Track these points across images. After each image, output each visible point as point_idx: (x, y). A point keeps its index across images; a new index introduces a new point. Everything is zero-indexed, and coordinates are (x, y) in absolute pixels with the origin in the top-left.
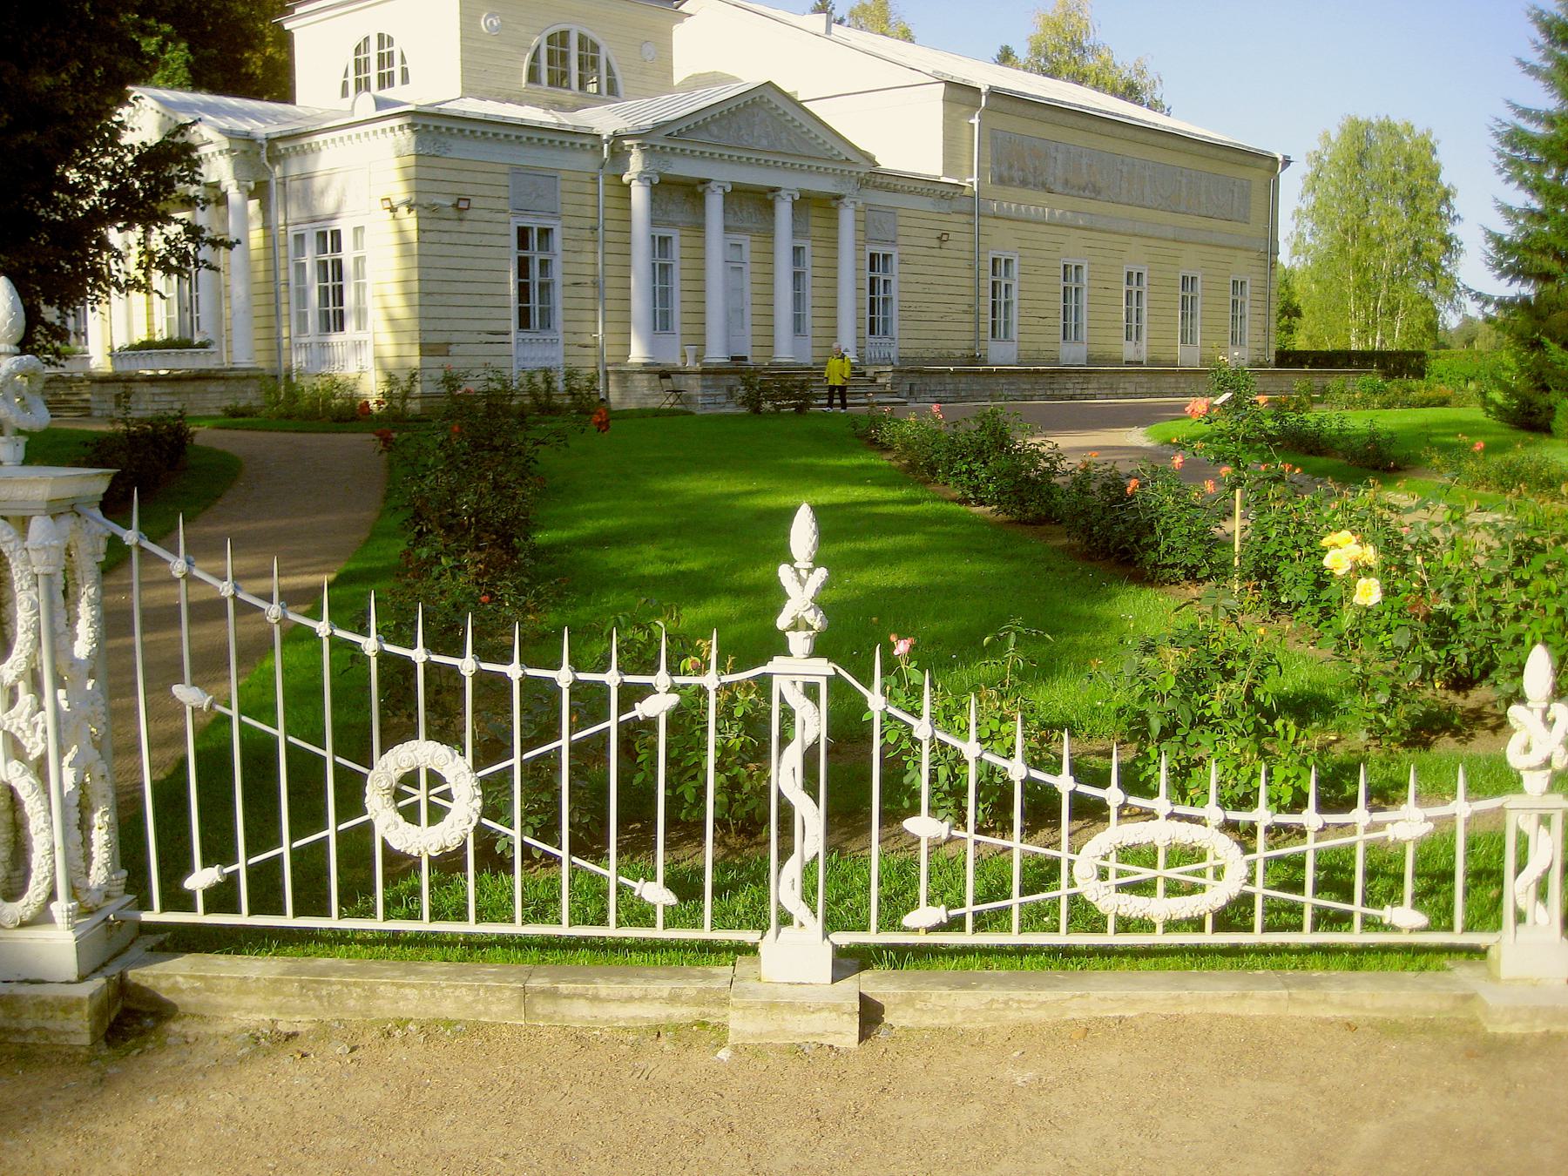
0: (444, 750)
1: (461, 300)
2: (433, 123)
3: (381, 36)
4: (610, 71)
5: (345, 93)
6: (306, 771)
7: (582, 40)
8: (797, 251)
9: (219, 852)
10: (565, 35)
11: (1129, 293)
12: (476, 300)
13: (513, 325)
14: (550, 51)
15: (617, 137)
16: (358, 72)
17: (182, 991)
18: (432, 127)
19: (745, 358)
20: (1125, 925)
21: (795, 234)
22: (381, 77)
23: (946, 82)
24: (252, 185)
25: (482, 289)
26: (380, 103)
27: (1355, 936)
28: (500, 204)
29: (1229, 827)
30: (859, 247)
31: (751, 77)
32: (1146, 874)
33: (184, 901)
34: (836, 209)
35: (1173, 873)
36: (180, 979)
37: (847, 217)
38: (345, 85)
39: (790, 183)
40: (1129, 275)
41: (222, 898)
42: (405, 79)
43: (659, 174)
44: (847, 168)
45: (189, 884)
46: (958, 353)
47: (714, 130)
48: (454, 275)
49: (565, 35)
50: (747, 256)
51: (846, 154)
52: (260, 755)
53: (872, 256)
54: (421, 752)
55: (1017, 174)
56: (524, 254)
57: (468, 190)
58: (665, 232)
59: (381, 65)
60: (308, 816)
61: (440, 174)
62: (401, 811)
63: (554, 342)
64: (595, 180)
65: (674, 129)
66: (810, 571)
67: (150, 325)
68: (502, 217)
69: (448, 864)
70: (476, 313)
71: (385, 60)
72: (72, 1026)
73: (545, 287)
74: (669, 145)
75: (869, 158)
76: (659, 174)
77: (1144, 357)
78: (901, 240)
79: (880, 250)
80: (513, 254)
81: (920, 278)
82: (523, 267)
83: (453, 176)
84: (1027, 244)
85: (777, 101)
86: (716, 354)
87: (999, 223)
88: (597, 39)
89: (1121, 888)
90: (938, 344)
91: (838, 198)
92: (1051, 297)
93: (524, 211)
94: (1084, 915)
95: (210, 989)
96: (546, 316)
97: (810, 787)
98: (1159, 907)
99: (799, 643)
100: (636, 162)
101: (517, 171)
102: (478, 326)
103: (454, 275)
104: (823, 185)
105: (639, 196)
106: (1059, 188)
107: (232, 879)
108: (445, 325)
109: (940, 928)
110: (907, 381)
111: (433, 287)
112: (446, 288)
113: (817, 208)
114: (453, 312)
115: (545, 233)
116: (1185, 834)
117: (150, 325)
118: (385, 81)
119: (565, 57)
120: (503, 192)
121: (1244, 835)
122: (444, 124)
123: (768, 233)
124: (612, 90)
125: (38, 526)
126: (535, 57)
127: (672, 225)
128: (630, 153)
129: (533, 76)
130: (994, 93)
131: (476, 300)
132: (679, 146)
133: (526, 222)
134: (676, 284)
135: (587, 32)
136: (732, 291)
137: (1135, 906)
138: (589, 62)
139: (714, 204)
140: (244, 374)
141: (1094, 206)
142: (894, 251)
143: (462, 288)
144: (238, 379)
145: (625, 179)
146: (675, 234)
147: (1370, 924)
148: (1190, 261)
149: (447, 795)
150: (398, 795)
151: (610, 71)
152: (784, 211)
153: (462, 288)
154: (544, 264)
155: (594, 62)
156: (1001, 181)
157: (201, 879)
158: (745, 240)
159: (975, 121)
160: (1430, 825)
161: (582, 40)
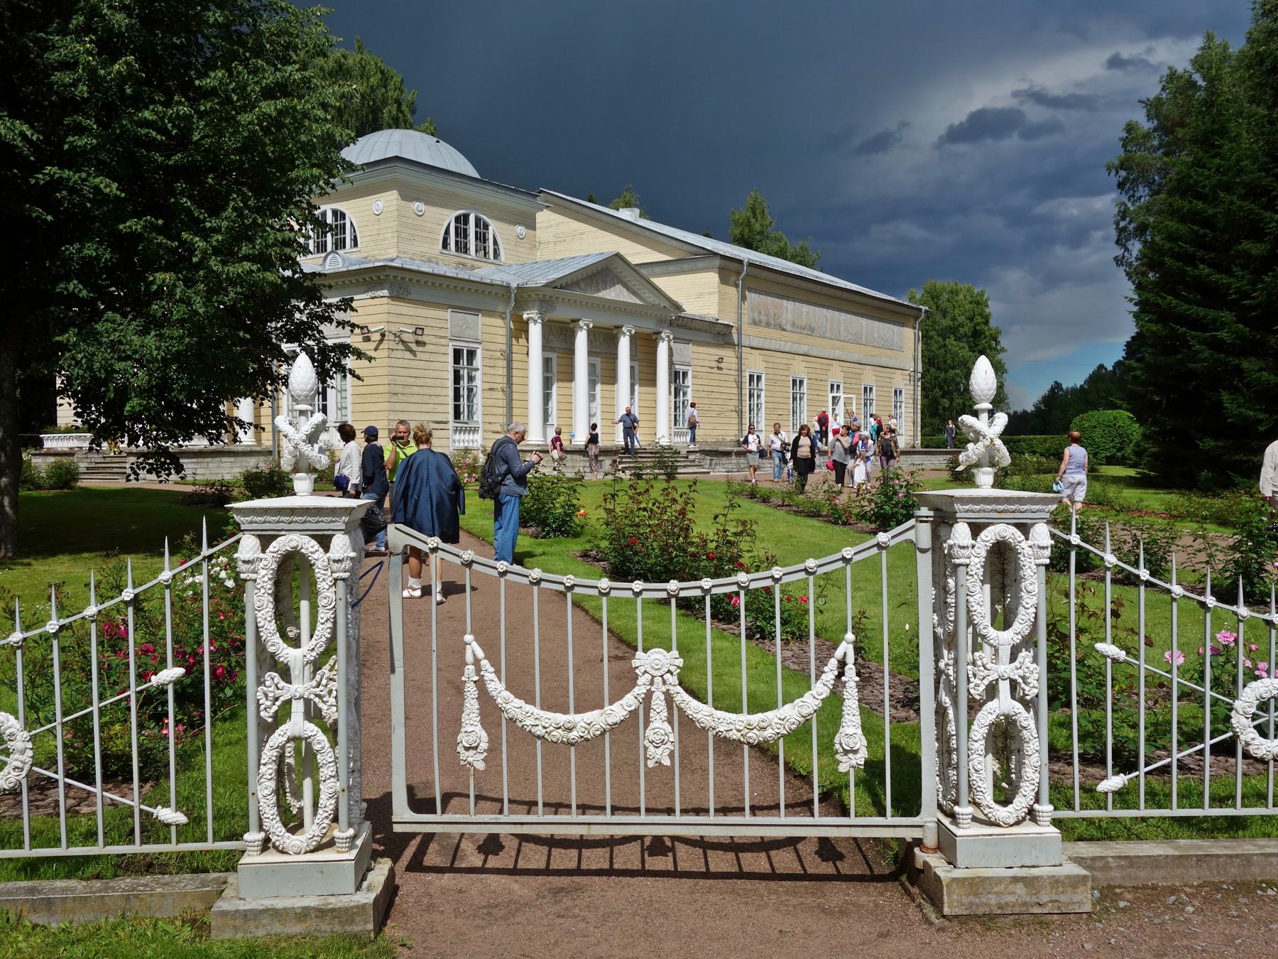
1: (414, 399)
4: (495, 243)
7: (478, 220)
8: (632, 368)
10: (466, 217)
12: (426, 399)
13: (451, 417)
14: (456, 228)
25: (431, 391)
33: (1098, 801)
36: (1110, 860)
41: (1124, 798)
46: (728, 439)
48: (411, 381)
55: (763, 318)
57: (422, 322)
63: (475, 430)
68: (443, 341)
70: (425, 408)
72: (1077, 898)
75: (678, 308)
81: (706, 388)
82: (457, 378)
90: (716, 433)
103: (411, 381)
106: (788, 327)
111: (399, 389)
112: (407, 390)
115: (471, 354)
126: (447, 232)
127: (552, 349)
129: (445, 245)
130: (751, 265)
131: (426, 399)
138: (481, 238)
141: (811, 340)
143: (416, 390)
146: (553, 356)
151: (495, 243)
153: (416, 390)
157: (1114, 782)
158: (597, 361)
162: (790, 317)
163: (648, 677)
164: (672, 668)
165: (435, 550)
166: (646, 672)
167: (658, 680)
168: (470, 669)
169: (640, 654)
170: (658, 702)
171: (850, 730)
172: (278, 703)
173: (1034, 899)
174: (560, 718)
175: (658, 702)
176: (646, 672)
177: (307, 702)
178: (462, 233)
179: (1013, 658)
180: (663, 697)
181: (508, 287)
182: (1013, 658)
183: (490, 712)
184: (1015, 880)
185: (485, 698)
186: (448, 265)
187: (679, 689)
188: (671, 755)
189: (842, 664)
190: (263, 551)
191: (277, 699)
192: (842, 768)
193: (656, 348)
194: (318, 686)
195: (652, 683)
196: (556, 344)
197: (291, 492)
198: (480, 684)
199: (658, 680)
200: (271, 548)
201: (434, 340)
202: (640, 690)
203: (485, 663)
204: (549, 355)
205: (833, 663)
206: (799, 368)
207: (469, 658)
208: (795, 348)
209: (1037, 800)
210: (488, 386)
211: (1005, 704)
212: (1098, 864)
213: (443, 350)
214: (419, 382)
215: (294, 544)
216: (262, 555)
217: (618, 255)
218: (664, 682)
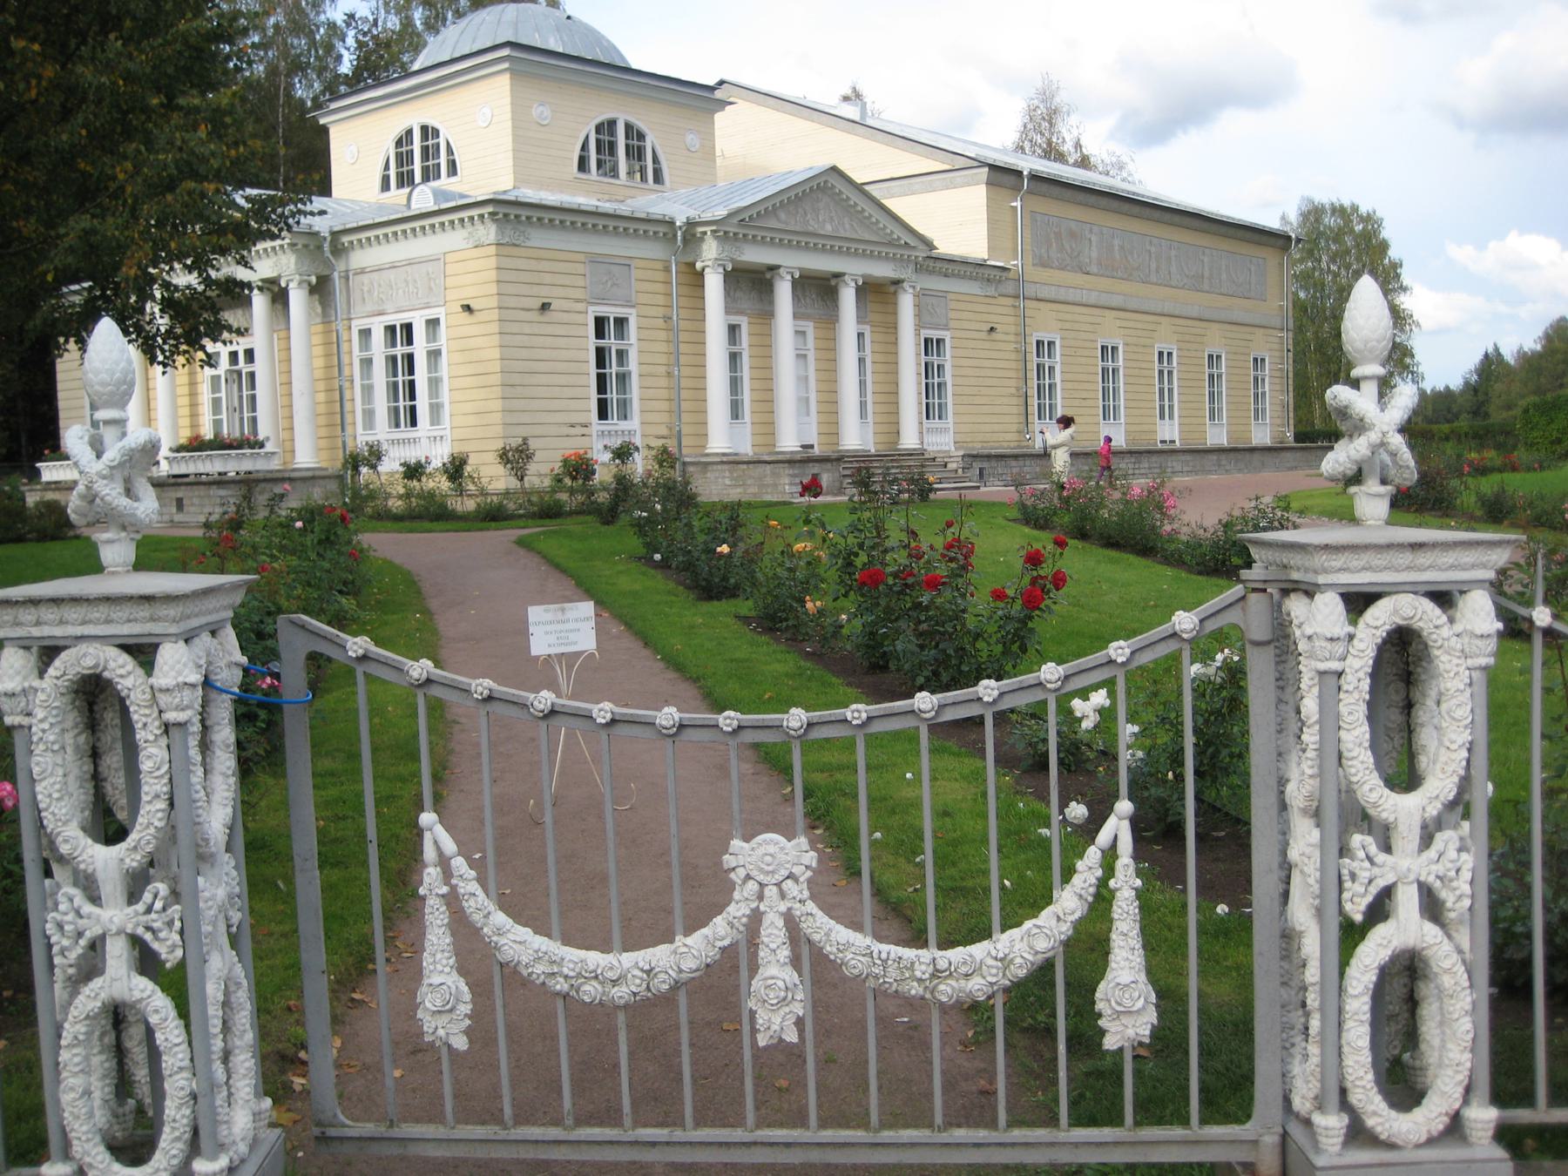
2: (513, 211)
3: (424, 129)
4: (655, 160)
5: (385, 186)
7: (629, 128)
10: (612, 123)
11: (1161, 372)
12: (556, 392)
14: (598, 141)
15: (691, 224)
16: (400, 163)
18: (511, 214)
19: (812, 447)
21: (861, 319)
22: (425, 170)
24: (314, 279)
25: (563, 380)
26: (439, 195)
28: (579, 294)
31: (824, 162)
34: (895, 293)
37: (906, 304)
39: (855, 269)
40: (1161, 354)
42: (453, 169)
43: (732, 260)
44: (906, 253)
47: (783, 216)
49: (612, 123)
53: (926, 340)
56: (602, 343)
58: (735, 319)
64: (667, 270)
65: (746, 215)
67: (194, 425)
68: (580, 307)
73: (623, 378)
74: (742, 231)
75: (929, 245)
76: (732, 260)
78: (952, 324)
79: (934, 334)
80: (592, 343)
82: (601, 355)
83: (533, 265)
84: (1067, 326)
85: (840, 186)
86: (789, 442)
87: (1041, 305)
91: (897, 282)
92: (1090, 378)
96: (624, 406)
100: (710, 251)
101: (594, 260)
102: (560, 418)
104: (882, 271)
105: (714, 284)
106: (1094, 269)
108: (525, 418)
110: (977, 465)
111: (516, 379)
113: (878, 294)
114: (536, 404)
115: (621, 322)
117: (194, 425)
119: (612, 147)
120: (580, 282)
122: (524, 213)
123: (830, 319)
126: (584, 147)
127: (740, 313)
128: (702, 240)
129: (583, 165)
130: (1035, 177)
131: (556, 392)
132: (751, 232)
133: (603, 310)
134: (746, 373)
135: (633, 120)
136: (803, 380)
138: (635, 153)
139: (784, 292)
140: (310, 474)
142: (946, 335)
143: (544, 379)
144: (304, 479)
145: (699, 265)
148: (1216, 340)
151: (655, 160)
152: (848, 296)
153: (544, 379)
154: (621, 354)
156: (1043, 263)
158: (809, 327)
159: (1018, 204)
161: (629, 128)
162: (1094, 254)
163: (752, 886)
164: (797, 870)
165: (364, 658)
166: (749, 877)
167: (771, 892)
168: (431, 874)
169: (736, 844)
170: (773, 934)
171: (1125, 977)
172: (82, 942)
174: (594, 958)
175: (773, 934)
176: (749, 877)
177: (136, 941)
178: (606, 148)
179: (1427, 840)
180: (780, 923)
181: (671, 223)
182: (1427, 840)
183: (472, 950)
185: (461, 925)
186: (586, 195)
187: (811, 906)
188: (799, 1023)
189: (1110, 854)
190: (41, 674)
191: (80, 934)
194: (149, 910)
195: (761, 897)
197: (92, 565)
198: (453, 900)
199: (771, 892)
200: (51, 671)
202: (738, 910)
203: (459, 863)
204: (735, 319)
205: (1093, 854)
206: (1112, 331)
207: (429, 853)
208: (1105, 300)
209: (1466, 1101)
211: (1406, 928)
213: (579, 318)
215: (89, 662)
216: (36, 683)
217: (834, 169)
218: (783, 896)
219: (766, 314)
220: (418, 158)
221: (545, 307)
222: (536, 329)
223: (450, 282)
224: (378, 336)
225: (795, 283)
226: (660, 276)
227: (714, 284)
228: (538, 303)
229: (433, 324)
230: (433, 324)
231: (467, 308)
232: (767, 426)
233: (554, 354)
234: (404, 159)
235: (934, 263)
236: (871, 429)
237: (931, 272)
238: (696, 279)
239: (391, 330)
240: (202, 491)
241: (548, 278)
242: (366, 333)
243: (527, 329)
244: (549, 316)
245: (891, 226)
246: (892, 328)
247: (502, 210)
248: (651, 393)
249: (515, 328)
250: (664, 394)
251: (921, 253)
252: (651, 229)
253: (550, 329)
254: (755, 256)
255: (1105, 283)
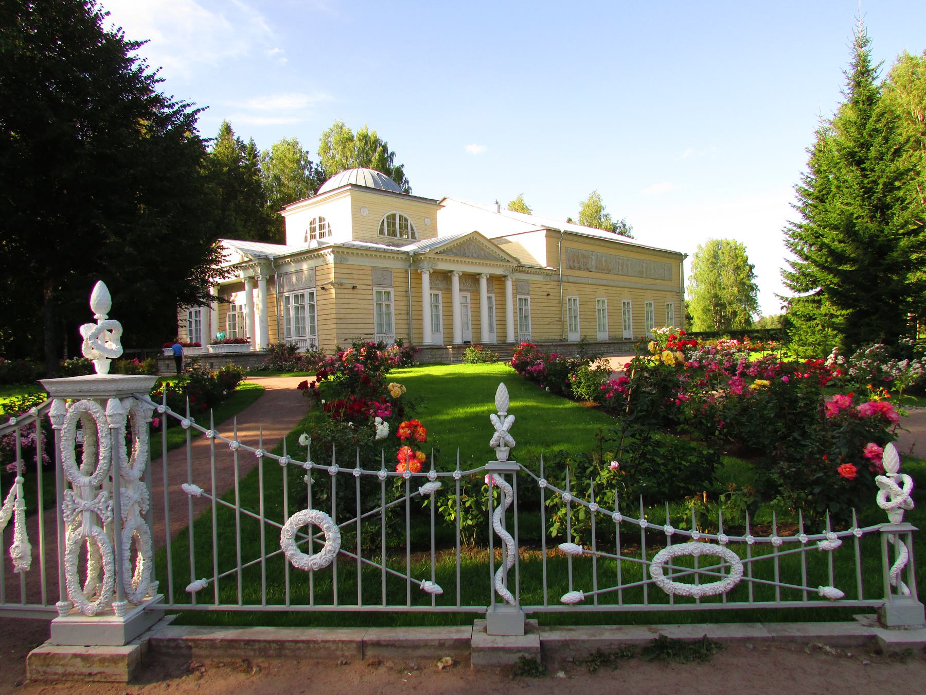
0: (321, 514)
1: (352, 321)
3: (321, 219)
5: (306, 241)
6: (251, 527)
7: (400, 216)
8: (489, 298)
9: (204, 571)
10: (394, 215)
12: (359, 321)
13: (376, 331)
17: (181, 648)
20: (679, 599)
21: (488, 292)
23: (549, 230)
27: (805, 603)
28: (370, 282)
29: (729, 544)
30: (514, 296)
32: (689, 571)
33: (187, 597)
35: (703, 570)
37: (509, 284)
38: (306, 237)
39: (486, 270)
41: (205, 595)
42: (330, 232)
44: (508, 264)
45: (189, 588)
48: (351, 311)
49: (394, 215)
50: (469, 300)
51: (508, 258)
52: (227, 517)
54: (309, 515)
55: (576, 265)
59: (320, 229)
60: (251, 553)
61: (345, 271)
62: (299, 547)
66: (506, 417)
68: (370, 287)
69: (323, 574)
70: (359, 326)
71: (322, 227)
72: (117, 671)
75: (517, 261)
77: (632, 337)
79: (523, 297)
83: (349, 271)
85: (479, 238)
88: (407, 217)
89: (675, 580)
91: (505, 276)
93: (379, 285)
94: (657, 594)
95: (197, 646)
97: (509, 528)
98: (696, 589)
99: (502, 454)
103: (351, 311)
104: (499, 272)
105: (426, 278)
107: (211, 585)
109: (580, 602)
111: (342, 316)
113: (497, 281)
115: (389, 293)
116: (709, 548)
118: (322, 235)
119: (394, 224)
121: (738, 547)
124: (413, 236)
125: (111, 403)
127: (439, 289)
129: (382, 232)
133: (379, 289)
137: (683, 588)
142: (528, 297)
143: (353, 316)
146: (440, 293)
147: (813, 596)
149: (323, 538)
150: (298, 538)
152: (484, 282)
155: (406, 227)
157: (196, 585)
158: (468, 295)
160: (840, 542)
161: (400, 216)
162: (594, 264)
173: (86, 670)
184: (75, 656)
192: (16, 571)
193: (504, 285)
196: (440, 286)
201: (363, 287)
208: (598, 282)
210: (398, 312)
212: (172, 644)
213: (370, 292)
214: (356, 311)
219: (449, 290)
220: (319, 227)
221: (354, 288)
222: (351, 296)
223: (318, 278)
224: (292, 301)
225: (460, 277)
226: (404, 275)
227: (426, 278)
228: (351, 286)
229: (312, 294)
230: (312, 294)
231: (323, 288)
232: (450, 334)
233: (359, 306)
234: (312, 230)
235: (521, 268)
236: (495, 335)
237: (520, 272)
238: (418, 276)
239: (296, 296)
240: (220, 360)
241: (356, 276)
242: (288, 298)
243: (347, 296)
244: (355, 291)
245: (502, 254)
246: (503, 294)
247: (336, 250)
248: (400, 321)
249: (342, 296)
250: (405, 322)
251: (515, 264)
252: (400, 256)
253: (357, 296)
254: (443, 266)
255: (599, 275)
